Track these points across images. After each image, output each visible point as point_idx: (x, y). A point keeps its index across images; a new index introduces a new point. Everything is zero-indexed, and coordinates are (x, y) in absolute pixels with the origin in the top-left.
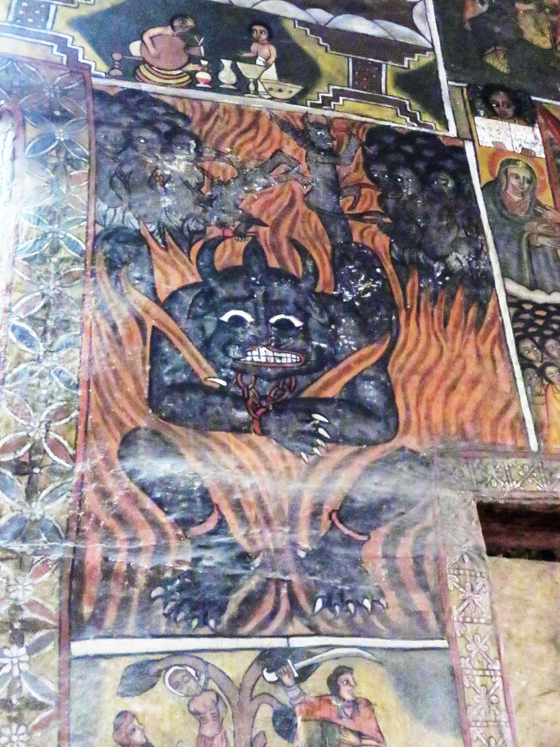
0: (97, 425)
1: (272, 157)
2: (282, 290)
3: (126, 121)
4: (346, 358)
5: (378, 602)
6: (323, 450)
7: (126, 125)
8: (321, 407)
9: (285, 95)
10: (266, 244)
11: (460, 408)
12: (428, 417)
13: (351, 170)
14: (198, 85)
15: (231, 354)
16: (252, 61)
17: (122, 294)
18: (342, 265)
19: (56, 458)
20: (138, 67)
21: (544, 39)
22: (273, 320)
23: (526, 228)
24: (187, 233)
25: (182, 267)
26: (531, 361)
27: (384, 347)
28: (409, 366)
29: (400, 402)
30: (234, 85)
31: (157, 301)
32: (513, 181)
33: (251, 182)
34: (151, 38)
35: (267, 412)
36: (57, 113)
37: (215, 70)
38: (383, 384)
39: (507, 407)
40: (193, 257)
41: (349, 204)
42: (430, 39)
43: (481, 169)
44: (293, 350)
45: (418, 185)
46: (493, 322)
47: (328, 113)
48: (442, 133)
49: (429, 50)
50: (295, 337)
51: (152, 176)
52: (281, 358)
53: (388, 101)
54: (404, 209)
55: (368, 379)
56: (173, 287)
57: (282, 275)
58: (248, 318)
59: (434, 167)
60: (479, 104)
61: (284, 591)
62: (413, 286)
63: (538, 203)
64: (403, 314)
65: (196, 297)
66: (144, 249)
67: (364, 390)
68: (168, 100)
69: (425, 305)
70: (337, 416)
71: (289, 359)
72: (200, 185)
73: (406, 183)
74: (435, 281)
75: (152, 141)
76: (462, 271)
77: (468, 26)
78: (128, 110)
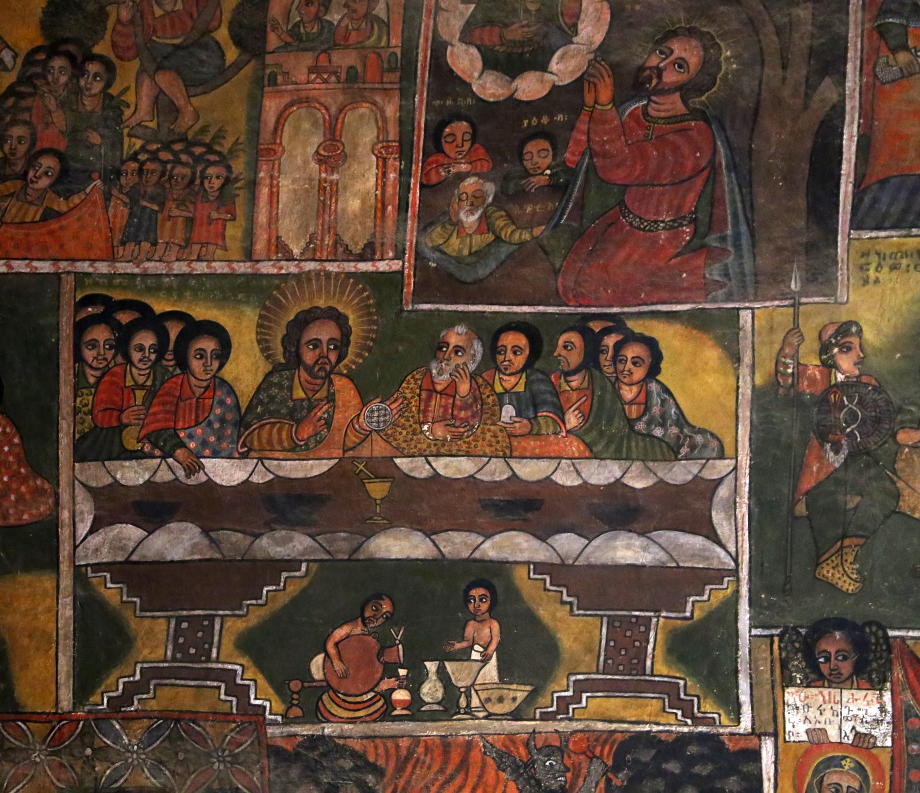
9: (507, 707)
16: (464, 656)
20: (320, 698)
30: (439, 703)
34: (337, 645)
42: (732, 549)
43: (780, 785)
47: (562, 726)
48: (728, 730)
53: (654, 687)
60: (797, 662)
68: (357, 745)
77: (801, 509)
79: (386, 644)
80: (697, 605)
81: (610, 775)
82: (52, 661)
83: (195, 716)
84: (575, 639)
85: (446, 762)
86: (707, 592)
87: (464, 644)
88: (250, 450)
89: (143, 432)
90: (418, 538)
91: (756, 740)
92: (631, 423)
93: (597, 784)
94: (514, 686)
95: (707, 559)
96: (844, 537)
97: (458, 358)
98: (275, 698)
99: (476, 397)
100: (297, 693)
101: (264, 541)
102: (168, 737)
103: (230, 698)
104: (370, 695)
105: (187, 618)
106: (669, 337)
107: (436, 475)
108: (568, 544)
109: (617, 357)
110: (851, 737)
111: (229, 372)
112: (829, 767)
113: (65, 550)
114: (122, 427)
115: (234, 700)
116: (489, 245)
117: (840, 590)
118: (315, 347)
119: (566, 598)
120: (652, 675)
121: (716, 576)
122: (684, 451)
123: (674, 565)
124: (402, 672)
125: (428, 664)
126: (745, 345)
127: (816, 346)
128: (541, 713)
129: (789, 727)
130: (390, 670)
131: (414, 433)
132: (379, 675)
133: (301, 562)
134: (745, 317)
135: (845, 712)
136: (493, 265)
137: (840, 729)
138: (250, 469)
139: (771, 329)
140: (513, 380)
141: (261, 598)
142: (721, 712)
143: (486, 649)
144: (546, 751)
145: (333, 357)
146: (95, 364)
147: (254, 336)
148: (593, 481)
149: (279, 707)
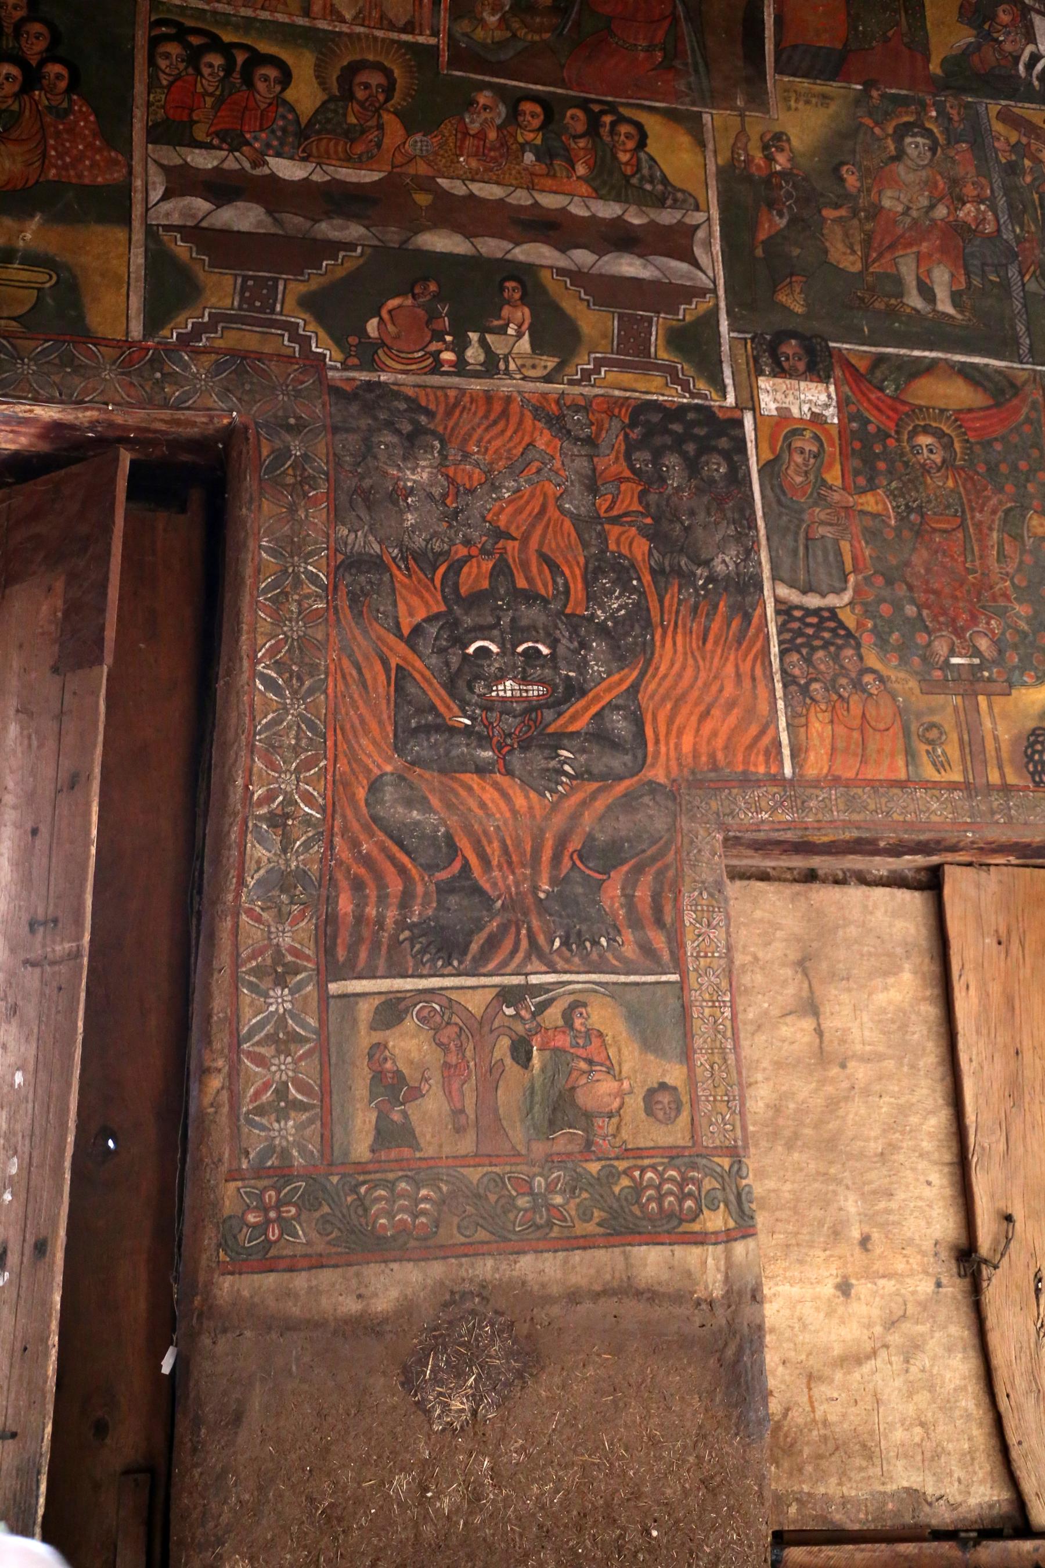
0: (344, 773)
2: (531, 614)
3: (365, 422)
5: (615, 941)
7: (363, 426)
11: (715, 734)
12: (678, 746)
16: (502, 330)
17: (365, 632)
18: (596, 579)
19: (307, 809)
20: (376, 352)
21: (852, 258)
22: (520, 649)
23: (806, 517)
24: (430, 555)
25: (427, 595)
26: (795, 677)
27: (635, 673)
31: (401, 637)
32: (798, 459)
33: (500, 487)
34: (390, 312)
35: (511, 751)
36: (292, 421)
37: (460, 346)
38: (634, 713)
39: (762, 732)
40: (438, 583)
42: (711, 275)
44: (541, 682)
45: (686, 474)
46: (757, 635)
47: (586, 391)
49: (710, 291)
52: (527, 691)
53: (658, 367)
55: (618, 708)
56: (418, 619)
57: (530, 597)
58: (494, 648)
59: (705, 448)
60: (765, 359)
61: (524, 932)
62: (673, 597)
63: (824, 482)
64: (659, 631)
66: (386, 578)
67: (613, 721)
68: (410, 392)
70: (583, 751)
71: (535, 691)
72: (444, 496)
74: (696, 591)
75: (394, 446)
77: (759, 252)
78: (369, 409)
79: (433, 315)
82: (124, 298)
83: (260, 356)
85: (488, 412)
87: (501, 322)
88: (309, 156)
89: (212, 129)
90: (458, 238)
92: (627, 179)
95: (691, 279)
96: (792, 275)
97: (486, 114)
98: (334, 348)
99: (503, 143)
101: (323, 226)
104: (420, 354)
105: (251, 278)
106: (653, 124)
107: (472, 195)
108: (583, 257)
109: (613, 132)
111: (290, 95)
113: (137, 210)
114: (193, 123)
116: (508, 39)
118: (366, 88)
121: (702, 292)
122: (669, 202)
124: (448, 338)
125: (470, 334)
126: (708, 136)
127: (759, 144)
129: (763, 405)
130: (438, 336)
131: (452, 162)
132: (428, 339)
134: (707, 118)
135: (802, 397)
136: (511, 53)
138: (310, 170)
139: (726, 129)
140: (532, 135)
143: (520, 327)
145: (381, 98)
146: (167, 70)
147: (312, 72)
148: (600, 215)
149: (340, 357)
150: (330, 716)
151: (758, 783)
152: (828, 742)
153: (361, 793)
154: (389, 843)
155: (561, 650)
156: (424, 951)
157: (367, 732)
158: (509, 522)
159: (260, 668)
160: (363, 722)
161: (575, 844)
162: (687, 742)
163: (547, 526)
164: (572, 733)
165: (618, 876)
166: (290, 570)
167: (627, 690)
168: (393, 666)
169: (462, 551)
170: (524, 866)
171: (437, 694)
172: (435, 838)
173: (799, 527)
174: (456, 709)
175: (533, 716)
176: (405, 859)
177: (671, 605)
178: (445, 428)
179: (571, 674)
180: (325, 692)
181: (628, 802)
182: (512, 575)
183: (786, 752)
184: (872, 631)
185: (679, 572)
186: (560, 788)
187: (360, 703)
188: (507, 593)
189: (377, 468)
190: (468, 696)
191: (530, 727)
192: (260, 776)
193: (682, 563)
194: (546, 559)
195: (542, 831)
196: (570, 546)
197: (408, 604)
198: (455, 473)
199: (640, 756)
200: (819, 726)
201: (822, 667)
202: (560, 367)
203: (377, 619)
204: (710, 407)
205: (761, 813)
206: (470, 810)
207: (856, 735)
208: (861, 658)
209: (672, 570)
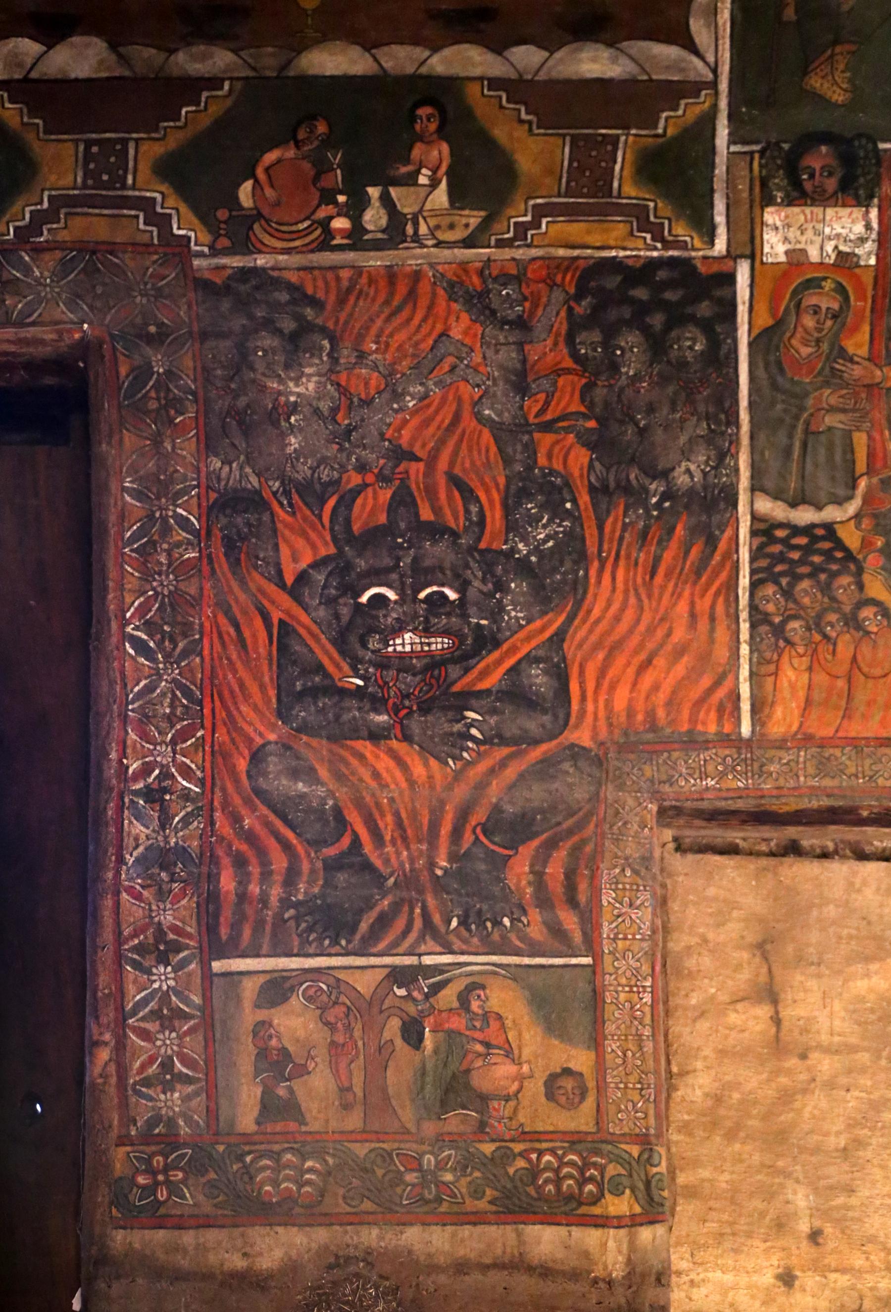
1: (432, 349)
2: (437, 551)
3: (239, 323)
4: (512, 636)
6: (474, 754)
8: (474, 702)
9: (458, 234)
10: (418, 488)
11: (656, 688)
12: (608, 704)
13: (546, 350)
14: (335, 242)
15: (370, 646)
16: (411, 180)
17: (243, 583)
19: (184, 783)
20: (251, 228)
22: (422, 595)
23: (810, 402)
24: (318, 487)
25: (313, 535)
26: (767, 614)
28: (593, 638)
29: (574, 687)
30: (383, 231)
33: (403, 394)
34: (267, 170)
36: (152, 329)
37: (357, 207)
38: (557, 665)
39: (717, 683)
40: (326, 519)
41: (535, 410)
43: (756, 308)
46: (722, 564)
47: (520, 254)
48: (701, 253)
49: (705, 85)
50: (448, 615)
51: (274, 408)
52: (429, 644)
53: (620, 209)
54: (619, 400)
55: (537, 660)
56: (303, 565)
57: (437, 531)
59: (678, 318)
61: (418, 911)
64: (596, 564)
65: (330, 574)
66: (266, 517)
67: (530, 676)
68: (293, 277)
69: (629, 545)
70: (494, 711)
71: (439, 644)
72: (335, 410)
73: (628, 355)
74: (647, 511)
75: (274, 351)
76: (691, 492)
78: (243, 304)
79: (322, 168)
80: (672, 121)
81: (572, 304)
83: (112, 248)
84: (534, 161)
85: (392, 293)
86: (682, 107)
90: (355, 51)
91: (731, 263)
93: (558, 314)
94: (467, 212)
100: (225, 222)
101: (181, 57)
102: (83, 269)
103: (149, 228)
104: (306, 224)
110: (833, 257)
112: (808, 288)
115: (155, 229)
117: (828, 101)
119: (524, 116)
120: (619, 196)
123: (645, 77)
124: (341, 199)
125: (371, 190)
128: (497, 240)
129: (767, 249)
130: (328, 197)
132: (316, 202)
133: (223, 80)
137: (822, 248)
141: (179, 120)
142: (694, 235)
143: (435, 171)
144: (502, 280)
150: (207, 682)
151: (706, 744)
152: (802, 694)
153: (242, 765)
154: (272, 817)
155: (472, 593)
156: (310, 929)
157: (247, 697)
158: (414, 439)
159: (129, 629)
160: (242, 686)
161: (480, 815)
162: (620, 701)
163: (461, 440)
164: (480, 692)
165: (527, 851)
166: (157, 515)
167: (551, 639)
168: (275, 622)
169: (356, 479)
170: (420, 841)
171: (325, 652)
172: (323, 811)
173: (797, 418)
174: (346, 668)
175: (436, 672)
176: (289, 834)
177: (613, 531)
178: (337, 322)
179: (484, 622)
180: (200, 654)
181: (546, 769)
182: (415, 504)
183: (745, 706)
184: (881, 551)
185: (626, 489)
186: (465, 755)
187: (239, 665)
188: (409, 529)
189: (254, 381)
190: (361, 653)
191: (431, 686)
192: (134, 747)
193: (632, 477)
194: (456, 482)
195: (442, 803)
196: (488, 464)
197: (291, 547)
198: (348, 380)
199: (561, 716)
200: (792, 675)
201: (806, 601)
202: (485, 225)
203: (256, 567)
204: (690, 259)
205: (705, 779)
206: (361, 780)
207: (841, 683)
208: (861, 587)
209: (618, 486)
